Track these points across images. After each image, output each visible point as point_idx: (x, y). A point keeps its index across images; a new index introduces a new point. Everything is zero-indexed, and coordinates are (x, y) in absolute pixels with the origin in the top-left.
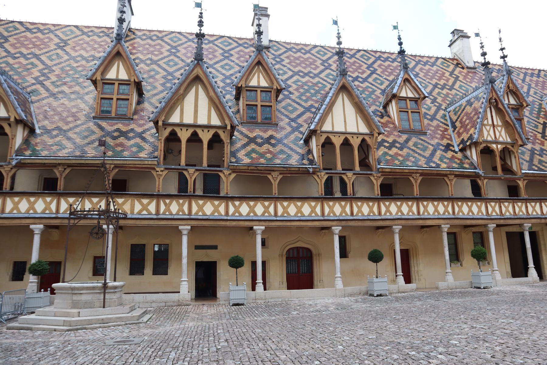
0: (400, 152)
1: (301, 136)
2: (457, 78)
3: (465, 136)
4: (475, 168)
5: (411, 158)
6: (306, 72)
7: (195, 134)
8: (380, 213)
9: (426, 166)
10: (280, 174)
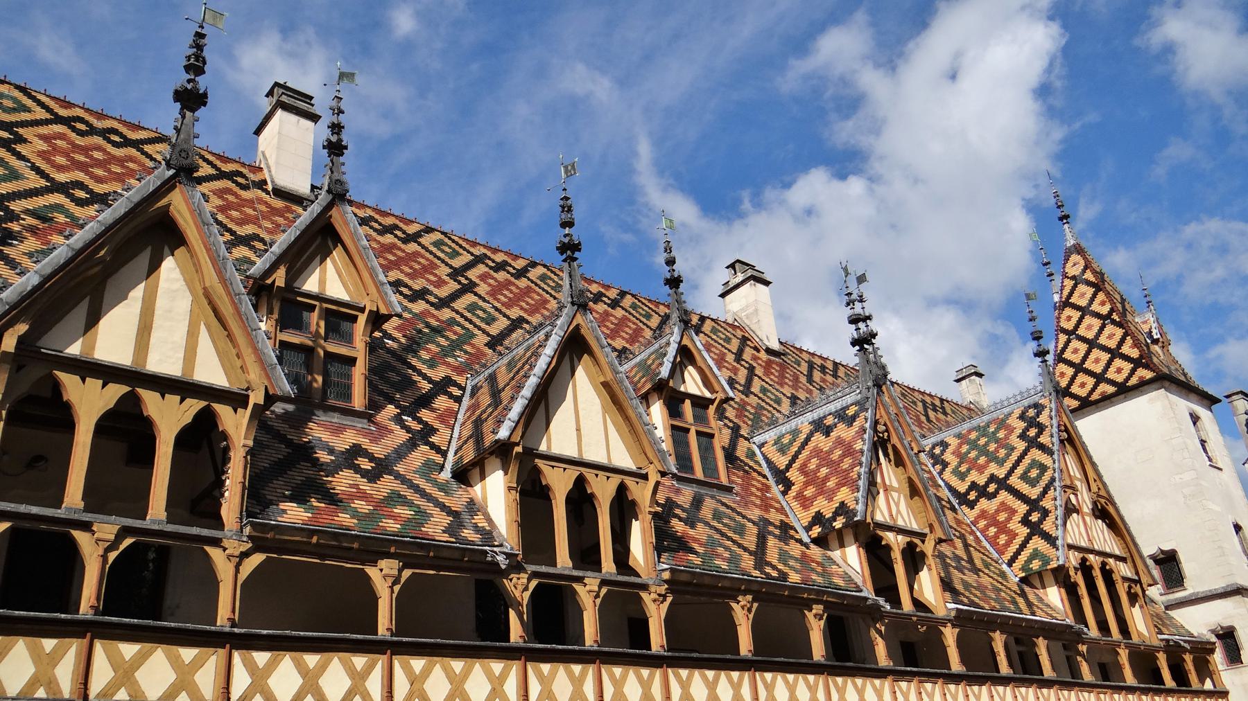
0: (691, 532)
1: (438, 459)
2: (751, 369)
3: (826, 507)
5: (720, 550)
6: (417, 287)
7: (130, 405)
9: (756, 573)
10: (406, 566)
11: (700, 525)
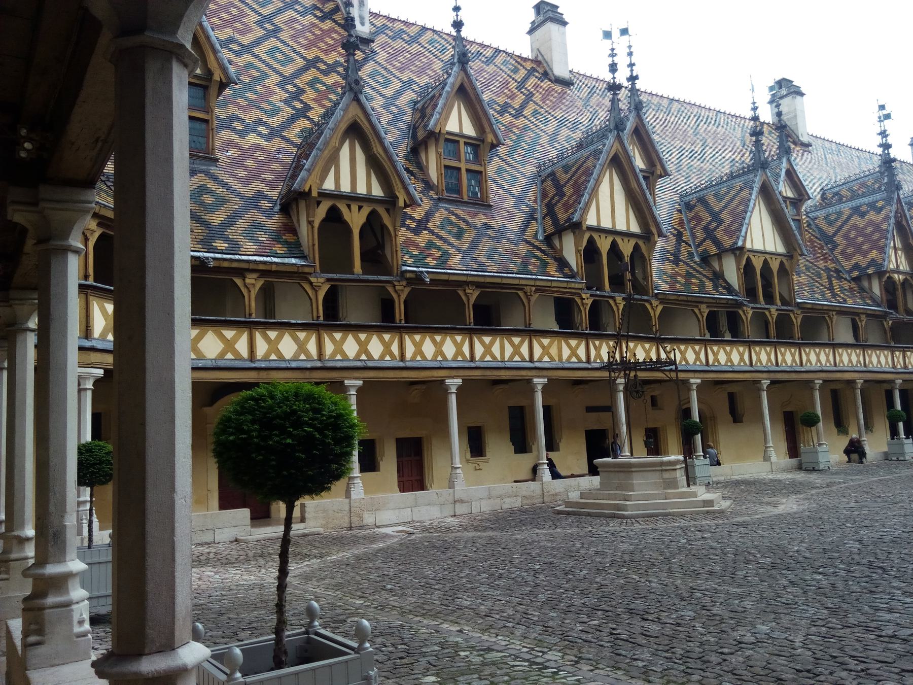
3: (863, 261)
4: (879, 306)
8: (865, 366)
9: (833, 300)
10: (708, 307)
11: (802, 275)
